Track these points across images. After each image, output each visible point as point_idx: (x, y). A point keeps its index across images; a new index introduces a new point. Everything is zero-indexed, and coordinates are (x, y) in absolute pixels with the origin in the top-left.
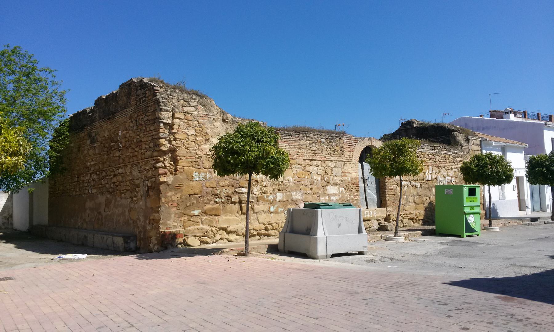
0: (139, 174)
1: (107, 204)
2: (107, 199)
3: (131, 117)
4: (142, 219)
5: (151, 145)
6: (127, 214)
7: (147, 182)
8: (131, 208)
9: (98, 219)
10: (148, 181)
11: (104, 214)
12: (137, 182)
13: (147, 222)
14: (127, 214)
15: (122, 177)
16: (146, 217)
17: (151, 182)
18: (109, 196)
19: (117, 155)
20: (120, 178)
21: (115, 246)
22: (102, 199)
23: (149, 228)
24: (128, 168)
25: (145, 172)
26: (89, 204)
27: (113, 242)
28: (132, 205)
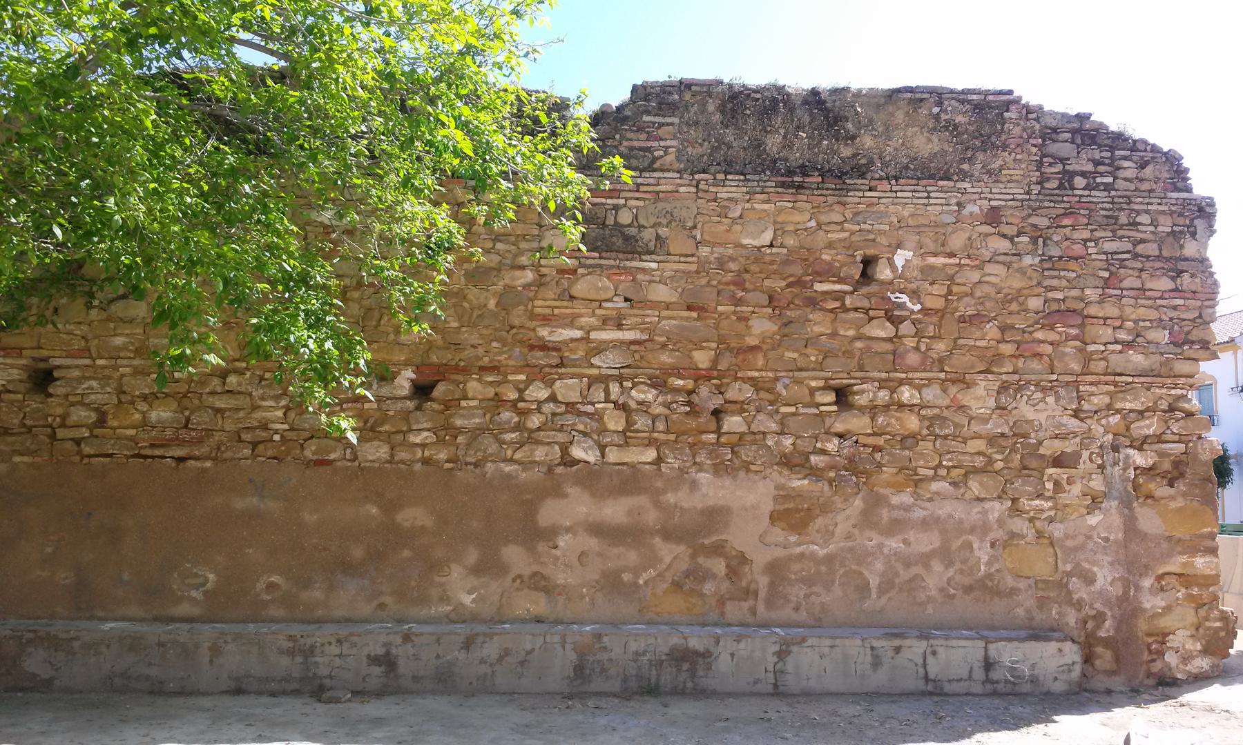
0: (1074, 423)
1: (792, 515)
2: (783, 495)
3: (993, 217)
4: (1105, 577)
5: (1163, 336)
6: (982, 553)
7: (1131, 451)
8: (1013, 535)
9: (697, 575)
10: (1140, 449)
11: (760, 557)
12: (1051, 448)
13: (1147, 583)
14: (982, 553)
15: (922, 418)
16: (1133, 567)
17: (1161, 455)
18: (796, 484)
19: (883, 334)
20: (913, 423)
21: (994, 675)
22: (750, 497)
23: (1152, 602)
24: (980, 390)
25: (1115, 419)
26: (572, 508)
27: (988, 665)
28: (1019, 525)
